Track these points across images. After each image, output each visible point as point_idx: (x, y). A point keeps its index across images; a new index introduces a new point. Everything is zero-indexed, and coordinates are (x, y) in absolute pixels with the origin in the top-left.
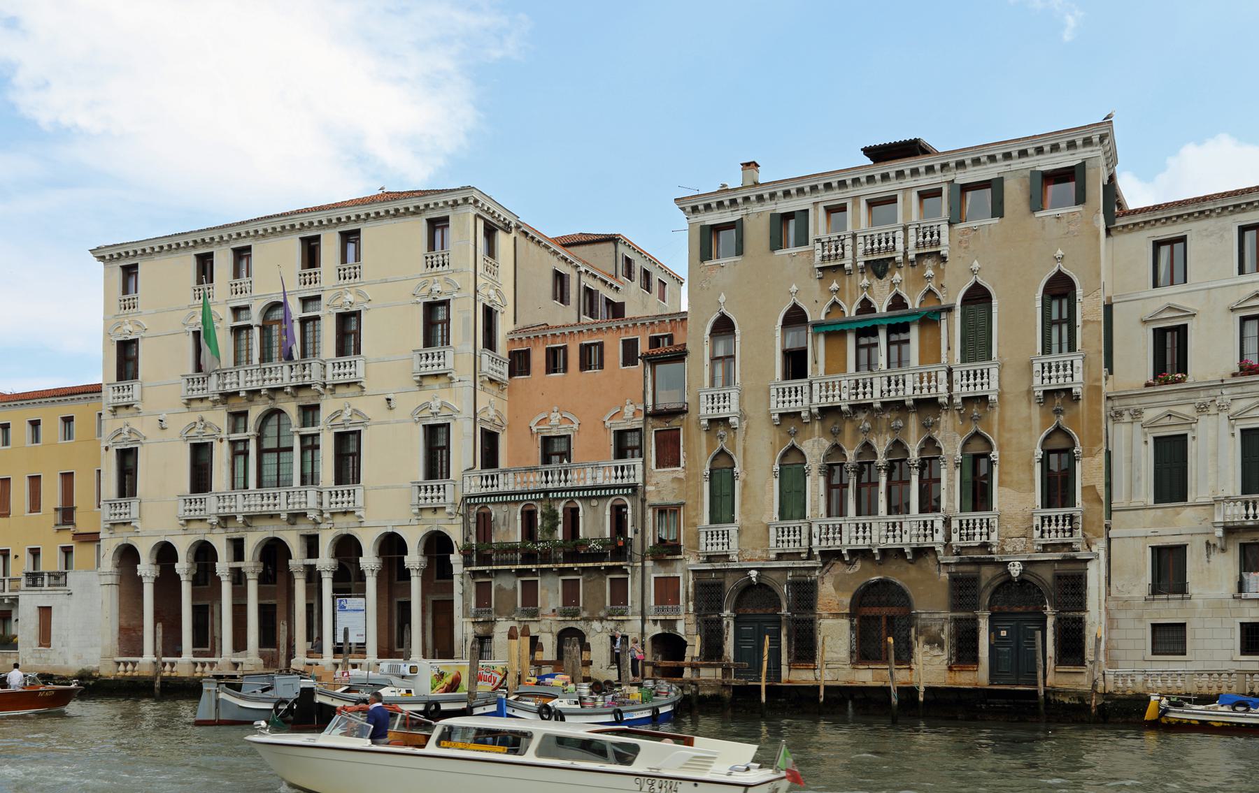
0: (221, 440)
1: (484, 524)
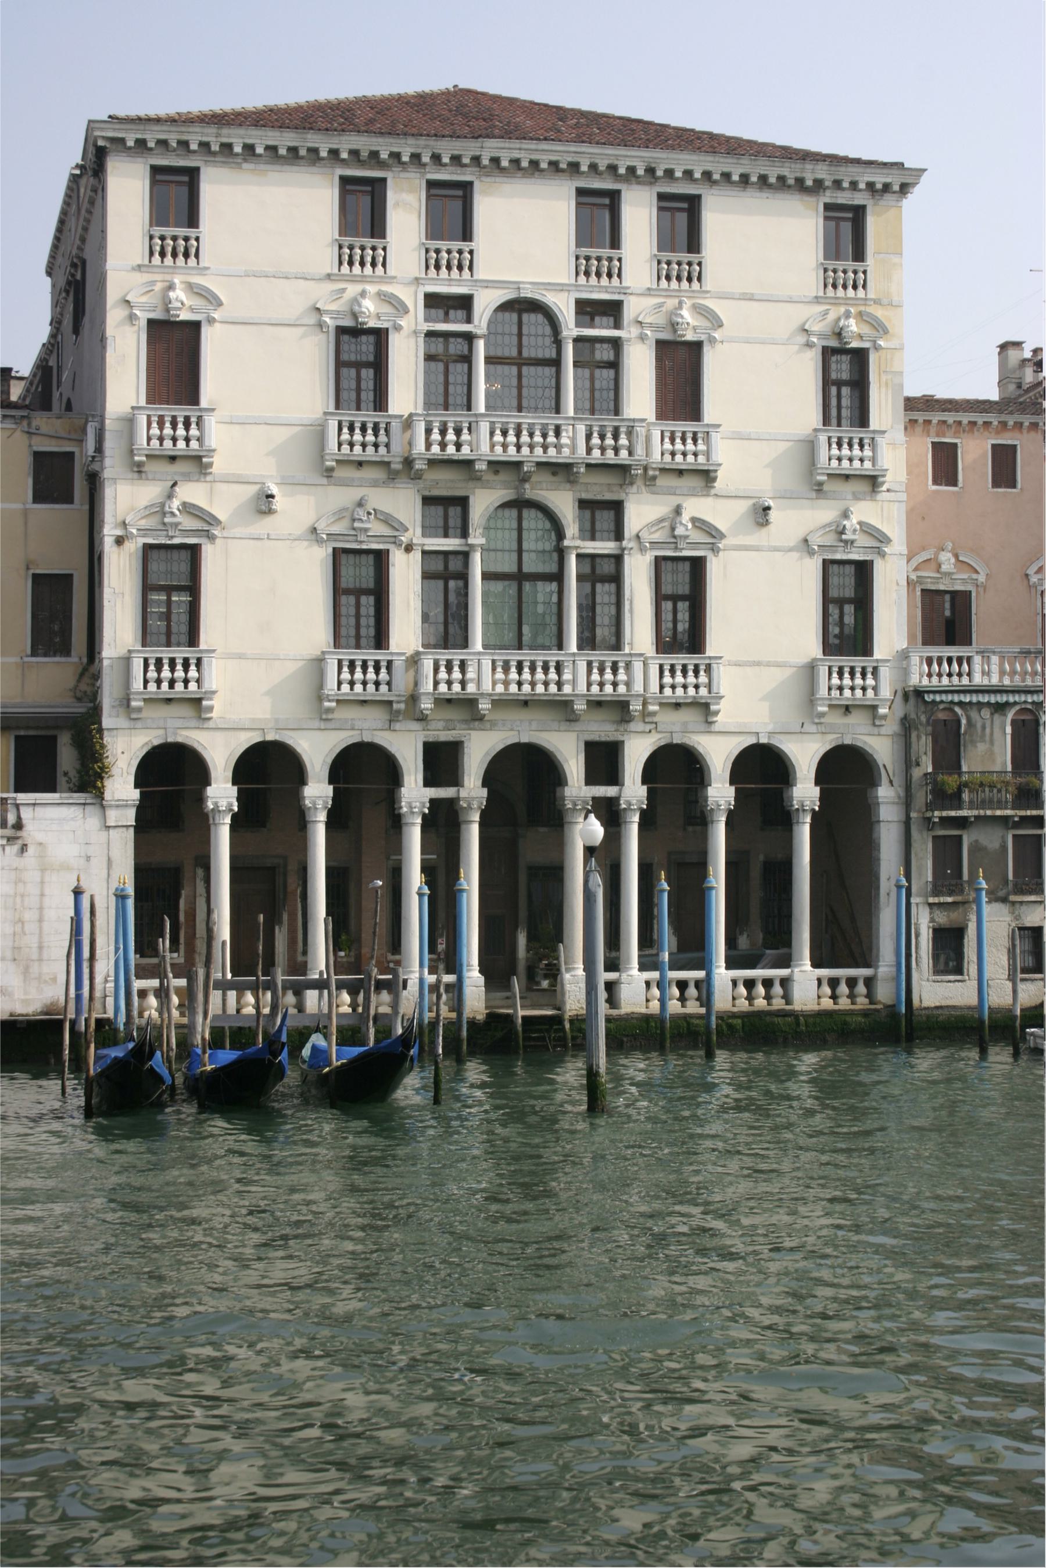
0: (409, 549)
1: (949, 740)
